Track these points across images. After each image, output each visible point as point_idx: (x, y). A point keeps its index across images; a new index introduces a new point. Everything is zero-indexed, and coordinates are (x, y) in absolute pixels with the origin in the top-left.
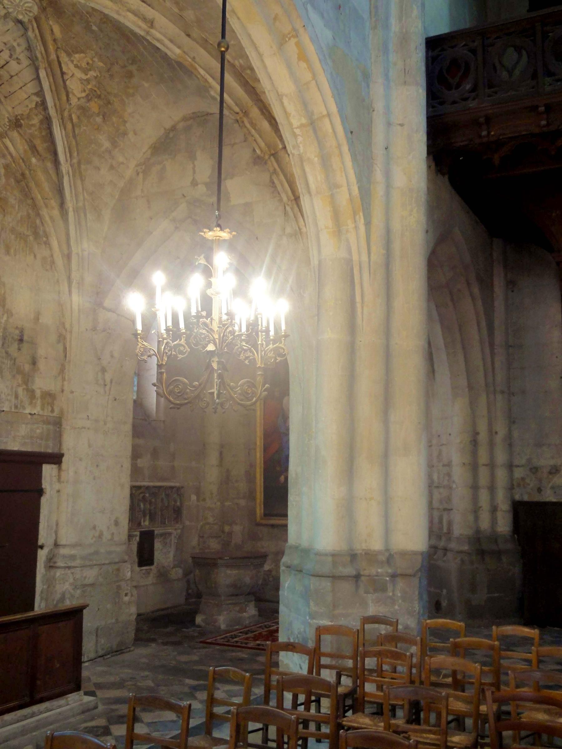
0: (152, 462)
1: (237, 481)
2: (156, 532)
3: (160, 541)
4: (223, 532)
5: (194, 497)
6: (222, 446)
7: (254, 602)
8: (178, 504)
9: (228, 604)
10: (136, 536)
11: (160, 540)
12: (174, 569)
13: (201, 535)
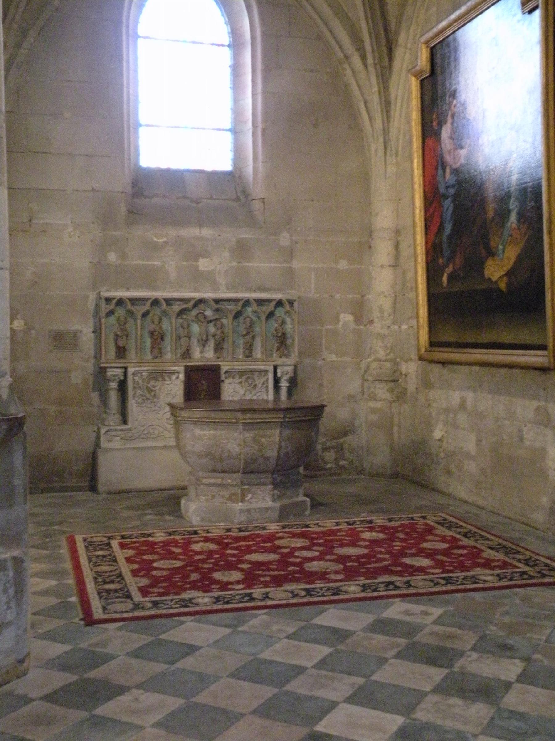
2: (224, 369)
3: (241, 383)
5: (347, 318)
6: (398, 232)
7: (270, 487)
9: (209, 485)
10: (178, 373)
13: (366, 377)
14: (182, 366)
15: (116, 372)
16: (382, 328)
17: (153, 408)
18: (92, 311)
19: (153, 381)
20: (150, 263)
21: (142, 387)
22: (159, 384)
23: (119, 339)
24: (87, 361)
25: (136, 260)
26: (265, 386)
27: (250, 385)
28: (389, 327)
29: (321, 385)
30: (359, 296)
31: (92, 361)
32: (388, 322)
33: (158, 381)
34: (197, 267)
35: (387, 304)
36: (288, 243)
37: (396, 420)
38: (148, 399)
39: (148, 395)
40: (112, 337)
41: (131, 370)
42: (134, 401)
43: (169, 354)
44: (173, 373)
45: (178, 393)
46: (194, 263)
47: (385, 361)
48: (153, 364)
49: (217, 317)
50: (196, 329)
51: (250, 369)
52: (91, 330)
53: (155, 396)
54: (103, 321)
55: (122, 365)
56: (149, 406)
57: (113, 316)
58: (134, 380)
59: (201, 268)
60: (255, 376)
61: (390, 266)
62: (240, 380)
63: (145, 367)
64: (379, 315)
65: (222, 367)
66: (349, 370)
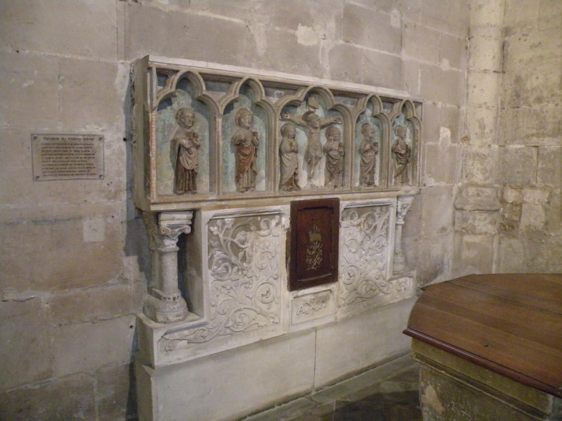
0: (341, 42)
1: (539, 100)
2: (343, 205)
3: (359, 225)
4: (503, 201)
5: (445, 132)
6: (507, 31)
8: (408, 140)
10: (280, 214)
11: (355, 223)
12: (394, 282)
13: (459, 206)
14: (286, 203)
15: (179, 219)
16: (481, 147)
17: (242, 280)
18: (123, 99)
19: (243, 232)
20: (227, 18)
21: (224, 246)
22: (251, 236)
23: (184, 154)
24: (115, 195)
25: (203, 10)
26: (385, 227)
27: (370, 226)
28: (489, 146)
29: (420, 218)
30: (456, 107)
31: (124, 196)
32: (489, 140)
33: (251, 231)
34: (294, 37)
35: (488, 117)
36: (398, 25)
37: (495, 257)
38: (233, 265)
39: (233, 259)
40: (167, 148)
41: (206, 215)
42: (210, 272)
43: (264, 182)
44: (272, 215)
45: (279, 250)
46: (291, 31)
47: (484, 186)
48: (244, 202)
49: (331, 119)
50: (302, 138)
51: (372, 203)
52: (122, 135)
53: (244, 259)
54: (153, 116)
55: (190, 206)
56: (233, 277)
57: (169, 108)
58: (211, 232)
59: (300, 41)
60: (376, 213)
61: (495, 72)
62: (359, 220)
63: (230, 207)
64: (478, 130)
65: (341, 202)
66: (444, 197)
